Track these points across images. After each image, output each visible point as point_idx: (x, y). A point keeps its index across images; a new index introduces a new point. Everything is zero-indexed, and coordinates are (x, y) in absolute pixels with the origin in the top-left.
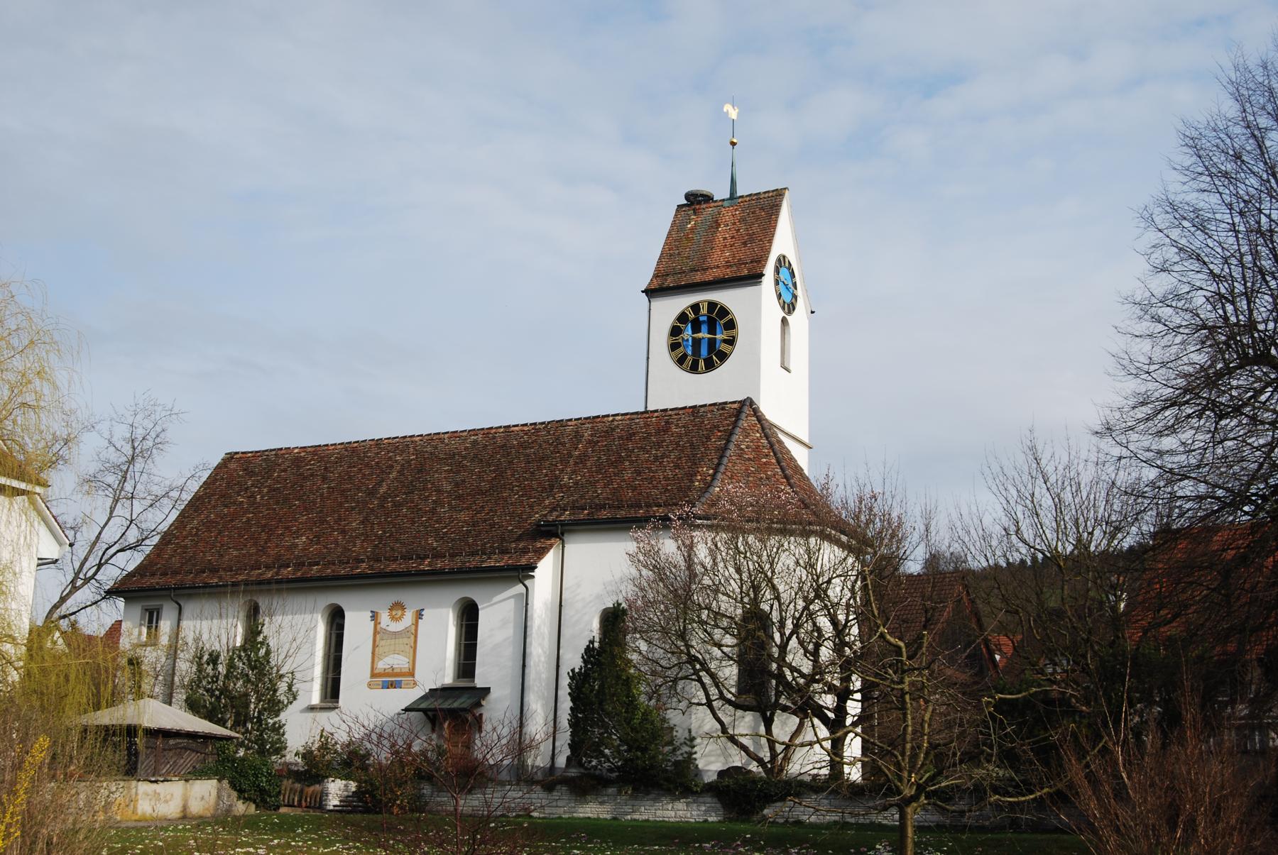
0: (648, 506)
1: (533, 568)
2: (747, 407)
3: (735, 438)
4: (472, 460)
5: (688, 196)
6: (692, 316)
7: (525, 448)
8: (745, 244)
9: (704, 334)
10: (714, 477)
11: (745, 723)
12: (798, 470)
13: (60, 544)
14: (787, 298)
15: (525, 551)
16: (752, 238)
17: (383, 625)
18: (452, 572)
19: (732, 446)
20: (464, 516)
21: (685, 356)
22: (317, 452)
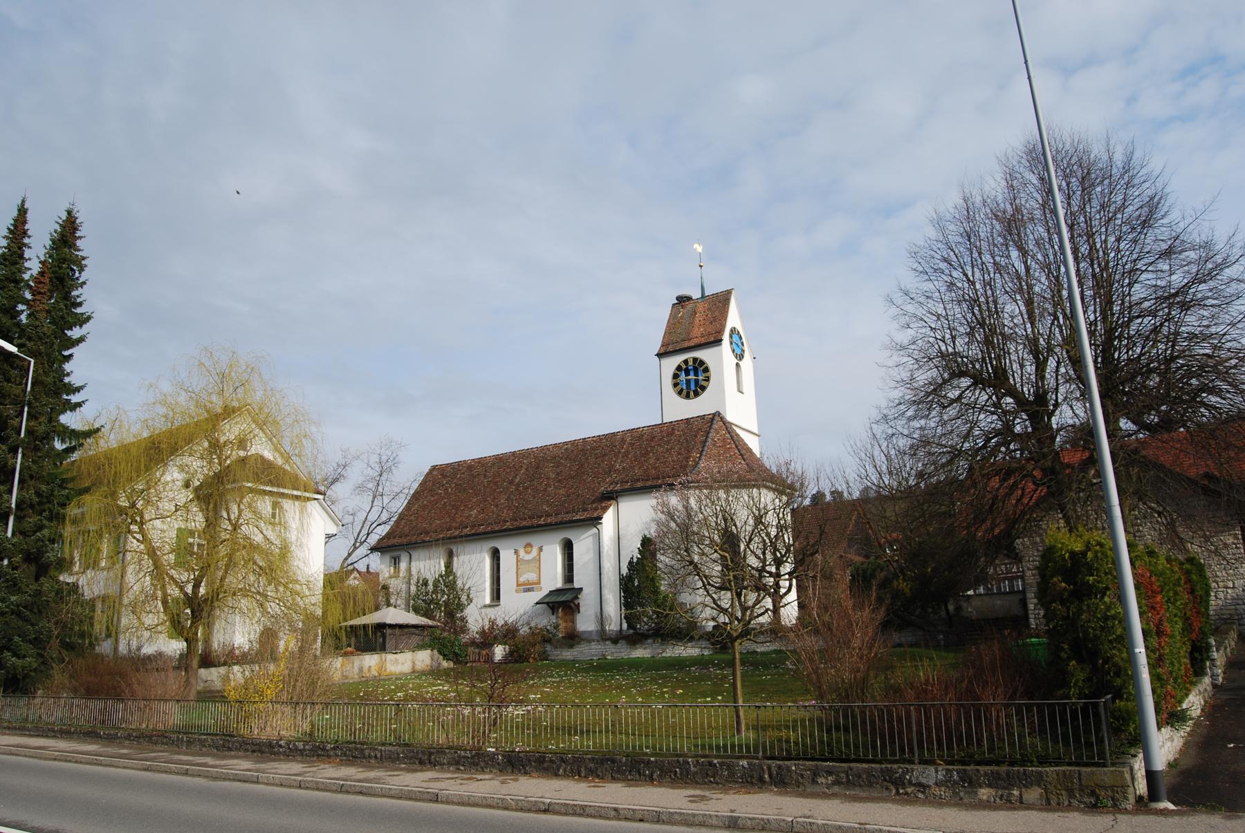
0: (664, 478)
1: (601, 518)
2: (717, 417)
3: (710, 435)
4: (566, 459)
5: (678, 298)
6: (684, 367)
7: (595, 450)
8: (711, 323)
9: (692, 377)
10: (700, 458)
11: (726, 599)
12: (749, 450)
13: (337, 525)
14: (738, 351)
15: (596, 509)
16: (715, 319)
17: (521, 557)
18: (556, 524)
19: (709, 440)
20: (562, 492)
21: (682, 390)
22: (481, 462)
